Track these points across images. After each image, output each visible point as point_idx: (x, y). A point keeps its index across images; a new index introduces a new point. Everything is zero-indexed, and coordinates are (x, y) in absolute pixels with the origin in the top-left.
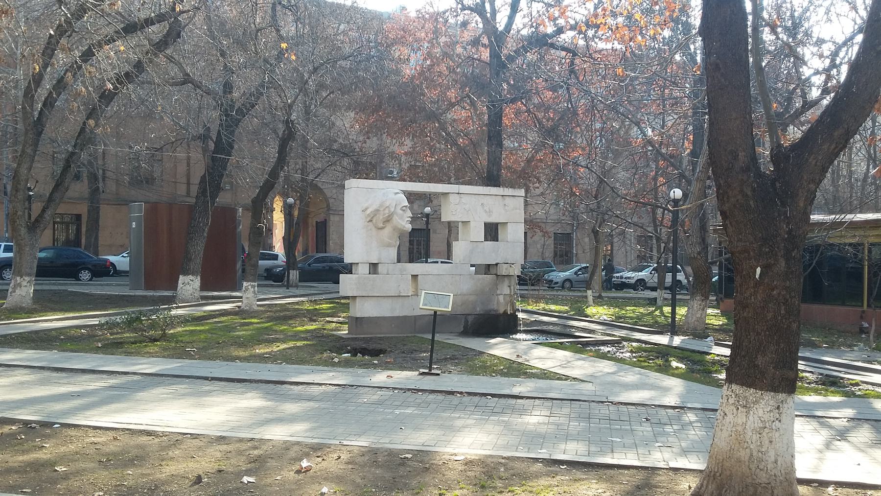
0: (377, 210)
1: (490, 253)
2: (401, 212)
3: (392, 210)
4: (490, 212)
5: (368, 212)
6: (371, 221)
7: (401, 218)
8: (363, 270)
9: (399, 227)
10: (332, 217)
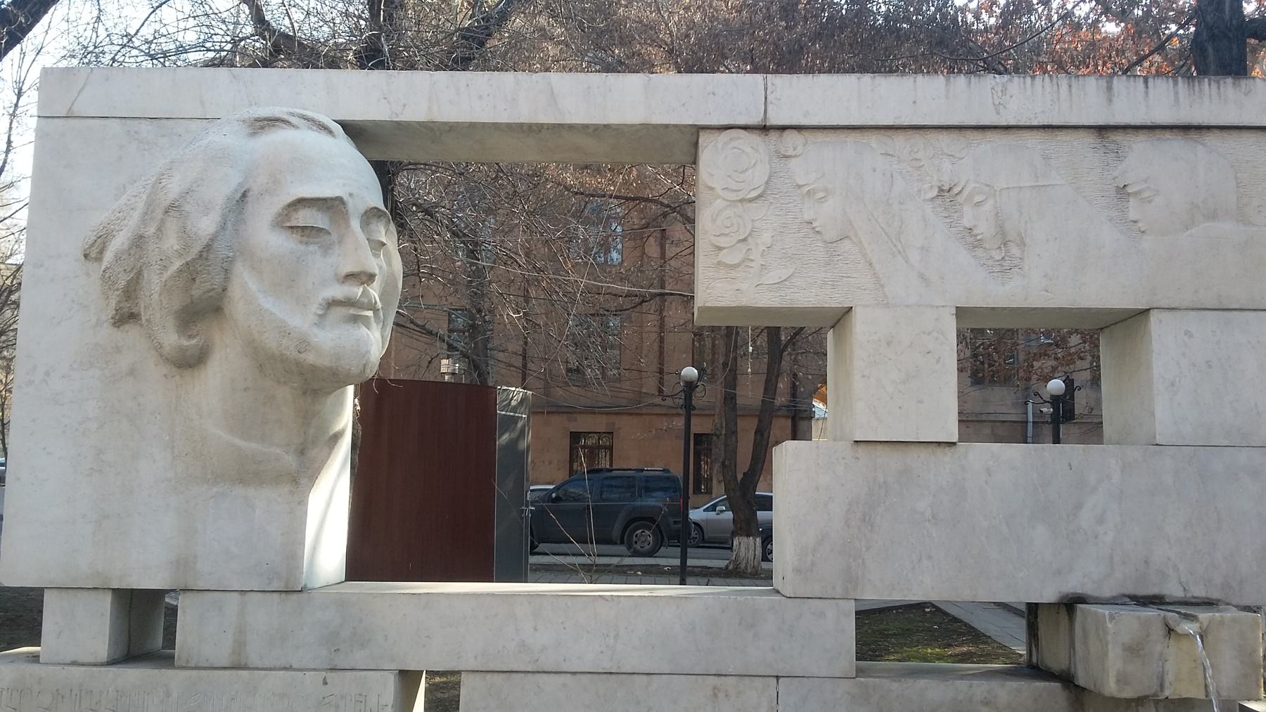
0: (139, 242)
3: (206, 225)
4: (1005, 247)
5: (109, 256)
6: (126, 317)
7: (287, 281)
8: (77, 631)
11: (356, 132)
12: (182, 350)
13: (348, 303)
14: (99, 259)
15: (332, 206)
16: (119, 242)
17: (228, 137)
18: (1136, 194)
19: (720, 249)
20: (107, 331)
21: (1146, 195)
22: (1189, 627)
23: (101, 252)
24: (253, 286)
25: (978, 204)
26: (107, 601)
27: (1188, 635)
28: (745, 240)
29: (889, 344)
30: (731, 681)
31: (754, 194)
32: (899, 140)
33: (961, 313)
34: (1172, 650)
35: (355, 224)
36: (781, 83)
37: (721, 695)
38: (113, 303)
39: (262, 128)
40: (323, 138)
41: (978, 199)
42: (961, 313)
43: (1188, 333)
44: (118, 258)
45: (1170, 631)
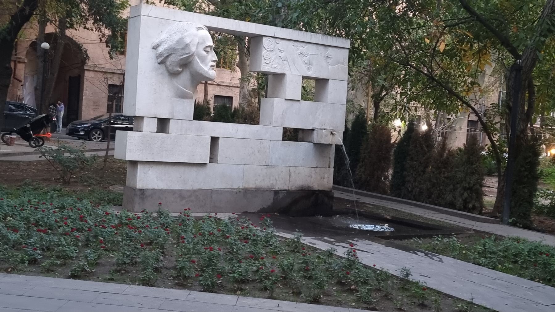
1: (301, 116)
5: (161, 49)
8: (149, 126)
9: (200, 72)
10: (87, 74)
11: (210, 29)
20: (157, 64)
24: (198, 61)
26: (156, 119)
32: (296, 43)
38: (161, 59)
44: (165, 50)
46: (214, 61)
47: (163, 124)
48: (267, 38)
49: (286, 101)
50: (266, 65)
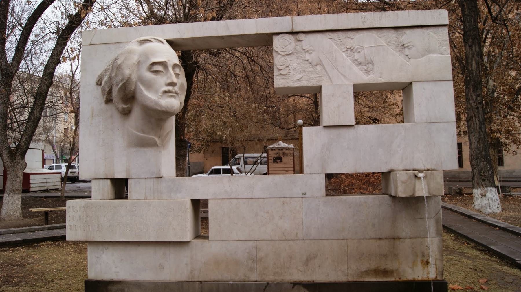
0: (110, 78)
2: (149, 75)
5: (103, 83)
6: (109, 101)
8: (101, 190)
12: (124, 109)
13: (169, 92)
14: (101, 85)
15: (163, 64)
16: (105, 79)
17: (134, 46)
18: (407, 47)
19: (280, 70)
20: (104, 105)
21: (410, 47)
22: (421, 175)
23: (101, 82)
25: (359, 52)
27: (420, 178)
28: (288, 67)
29: (333, 96)
30: (288, 199)
31: (290, 53)
33: (355, 86)
34: (417, 182)
35: (170, 69)
36: (297, 18)
37: (285, 204)
38: (105, 97)
39: (143, 43)
40: (161, 44)
41: (359, 50)
42: (355, 86)
43: (424, 89)
45: (416, 176)
46: (173, 84)
47: (120, 188)
48: (280, 36)
49: (328, 131)
50: (282, 77)
